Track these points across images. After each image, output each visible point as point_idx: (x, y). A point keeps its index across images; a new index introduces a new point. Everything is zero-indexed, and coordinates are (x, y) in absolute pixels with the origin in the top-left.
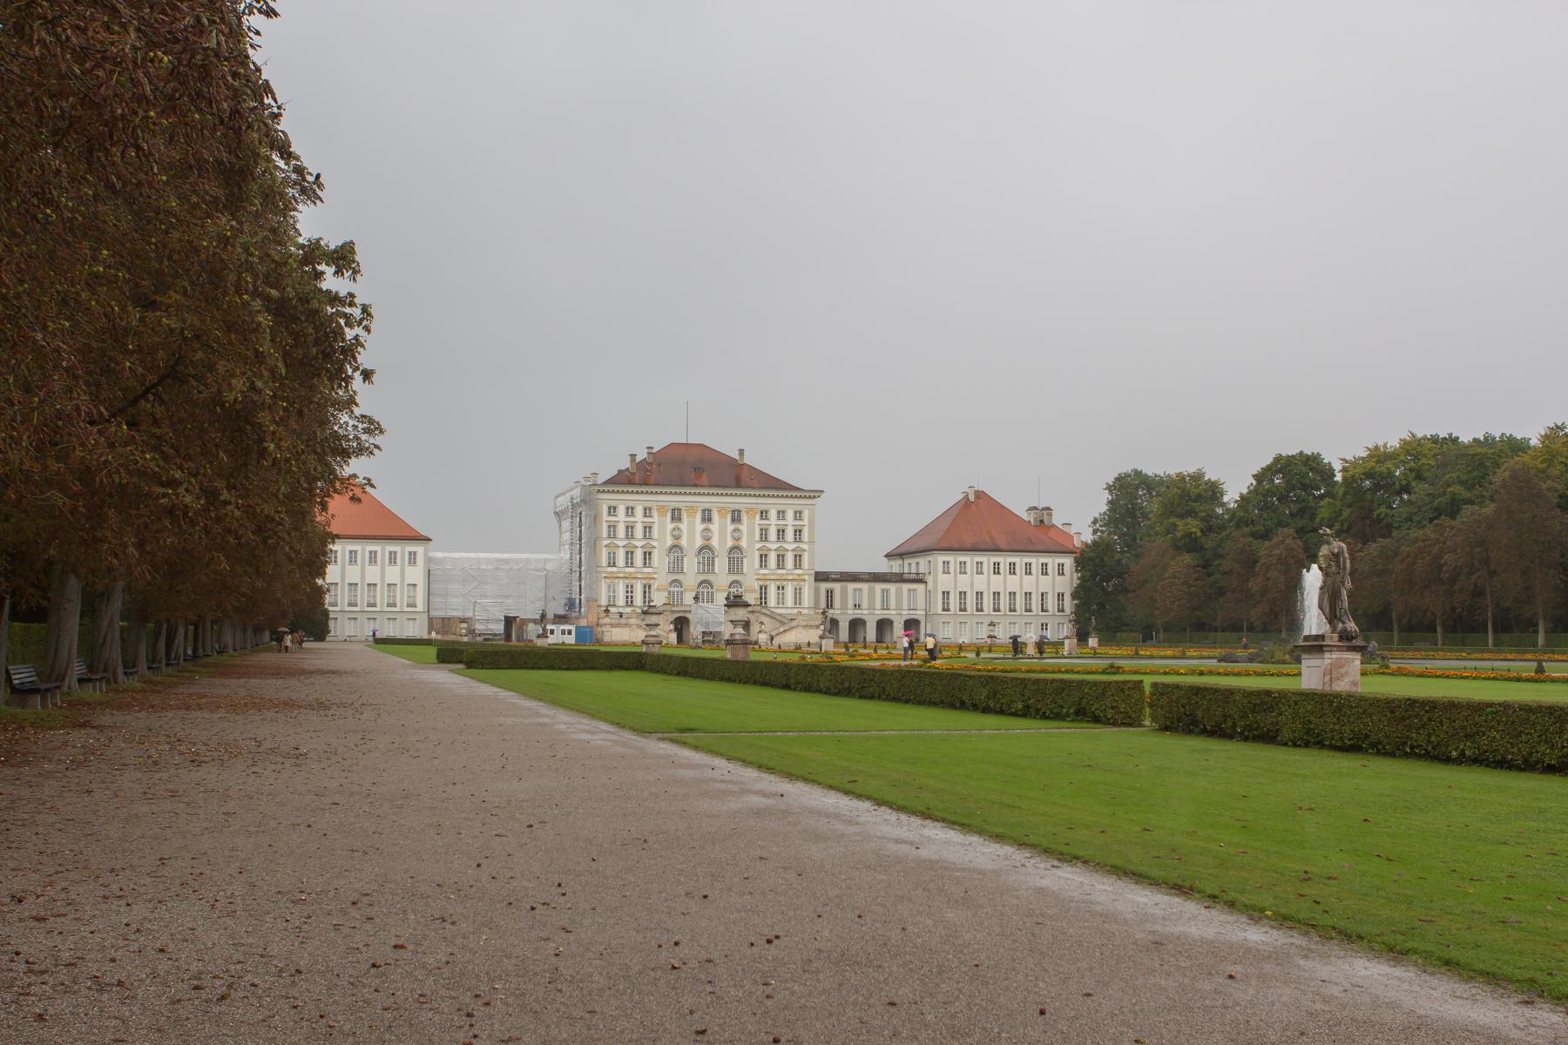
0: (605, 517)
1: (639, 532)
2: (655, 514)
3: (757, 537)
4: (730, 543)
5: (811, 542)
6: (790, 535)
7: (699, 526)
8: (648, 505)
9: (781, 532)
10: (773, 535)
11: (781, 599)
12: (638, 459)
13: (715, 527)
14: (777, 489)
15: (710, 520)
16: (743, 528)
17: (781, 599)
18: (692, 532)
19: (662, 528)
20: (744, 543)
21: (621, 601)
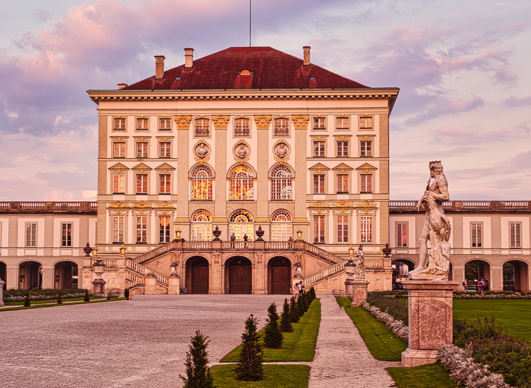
0: (110, 133)
1: (154, 150)
2: (174, 126)
3: (310, 153)
4: (272, 161)
5: (385, 157)
6: (354, 149)
7: (232, 141)
8: (165, 114)
9: (343, 145)
10: (331, 149)
11: (343, 234)
12: (169, 65)
13: (252, 141)
14: (333, 88)
15: (246, 132)
16: (291, 141)
17: (343, 234)
18: (222, 149)
19: (183, 142)
20: (291, 161)
21: (131, 239)
